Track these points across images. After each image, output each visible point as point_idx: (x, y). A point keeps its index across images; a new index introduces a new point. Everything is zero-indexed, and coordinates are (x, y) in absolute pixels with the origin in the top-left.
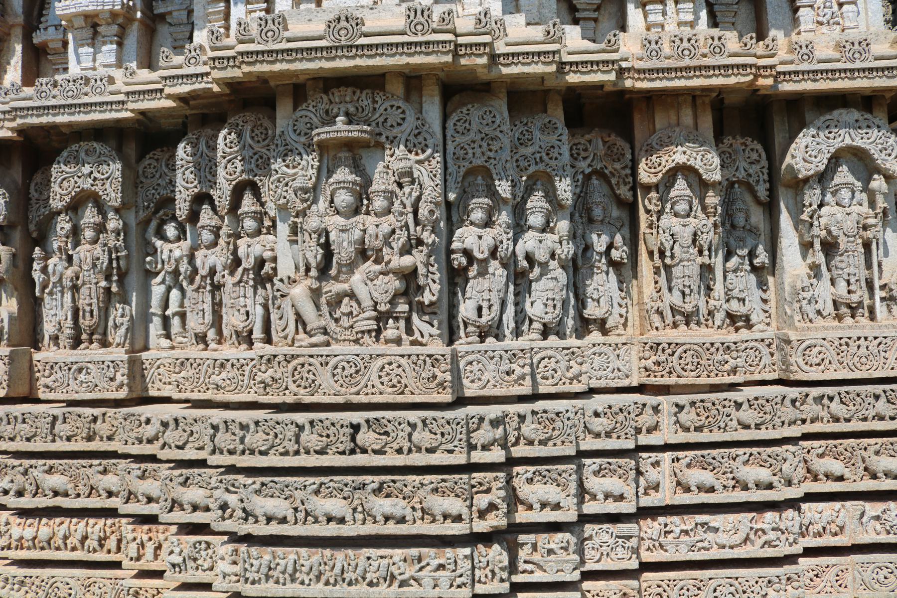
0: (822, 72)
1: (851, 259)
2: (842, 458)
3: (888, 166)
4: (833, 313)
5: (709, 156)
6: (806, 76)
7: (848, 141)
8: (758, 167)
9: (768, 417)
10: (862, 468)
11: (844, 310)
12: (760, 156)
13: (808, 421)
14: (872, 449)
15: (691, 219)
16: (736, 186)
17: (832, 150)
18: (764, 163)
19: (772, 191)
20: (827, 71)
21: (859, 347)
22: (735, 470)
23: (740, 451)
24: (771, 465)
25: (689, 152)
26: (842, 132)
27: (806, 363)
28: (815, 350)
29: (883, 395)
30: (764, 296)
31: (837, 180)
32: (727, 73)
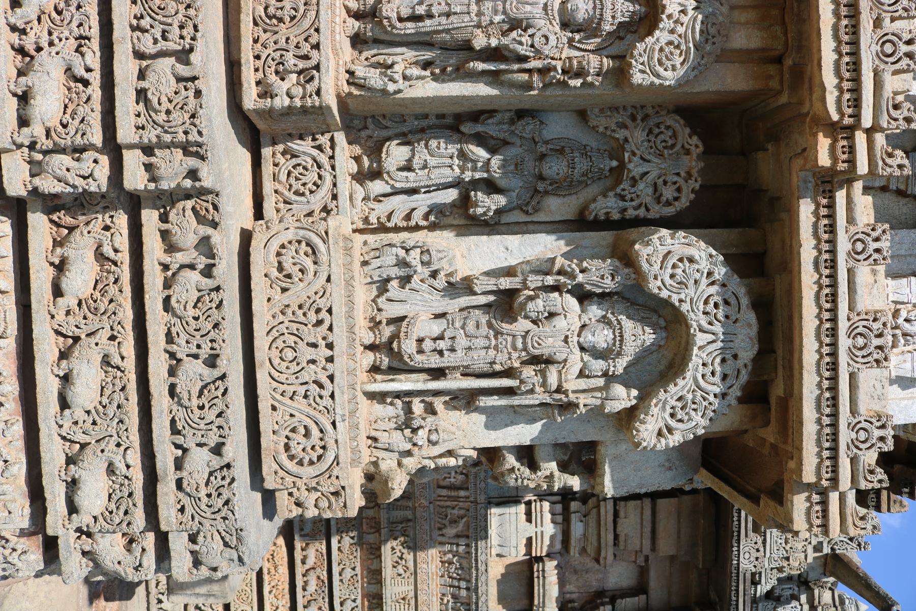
0: (833, 276)
1: (481, 342)
2: (97, 295)
3: (655, 410)
4: (383, 317)
5: (678, 60)
6: (825, 247)
7: (701, 339)
8: (648, 200)
9: (161, 118)
10: (77, 332)
11: (387, 331)
12: (668, 203)
13: (165, 226)
14: (112, 349)
15: (557, 28)
16: (615, 163)
17: (685, 308)
18: (657, 211)
19: (605, 224)
20: (834, 285)
21: (314, 345)
22: (54, 50)
23: (93, 59)
24: (65, 126)
25: (685, 19)
26: (718, 328)
27: (283, 246)
28: (308, 262)
29: (217, 373)
30: (417, 218)
31: (628, 325)
32: (844, 68)
